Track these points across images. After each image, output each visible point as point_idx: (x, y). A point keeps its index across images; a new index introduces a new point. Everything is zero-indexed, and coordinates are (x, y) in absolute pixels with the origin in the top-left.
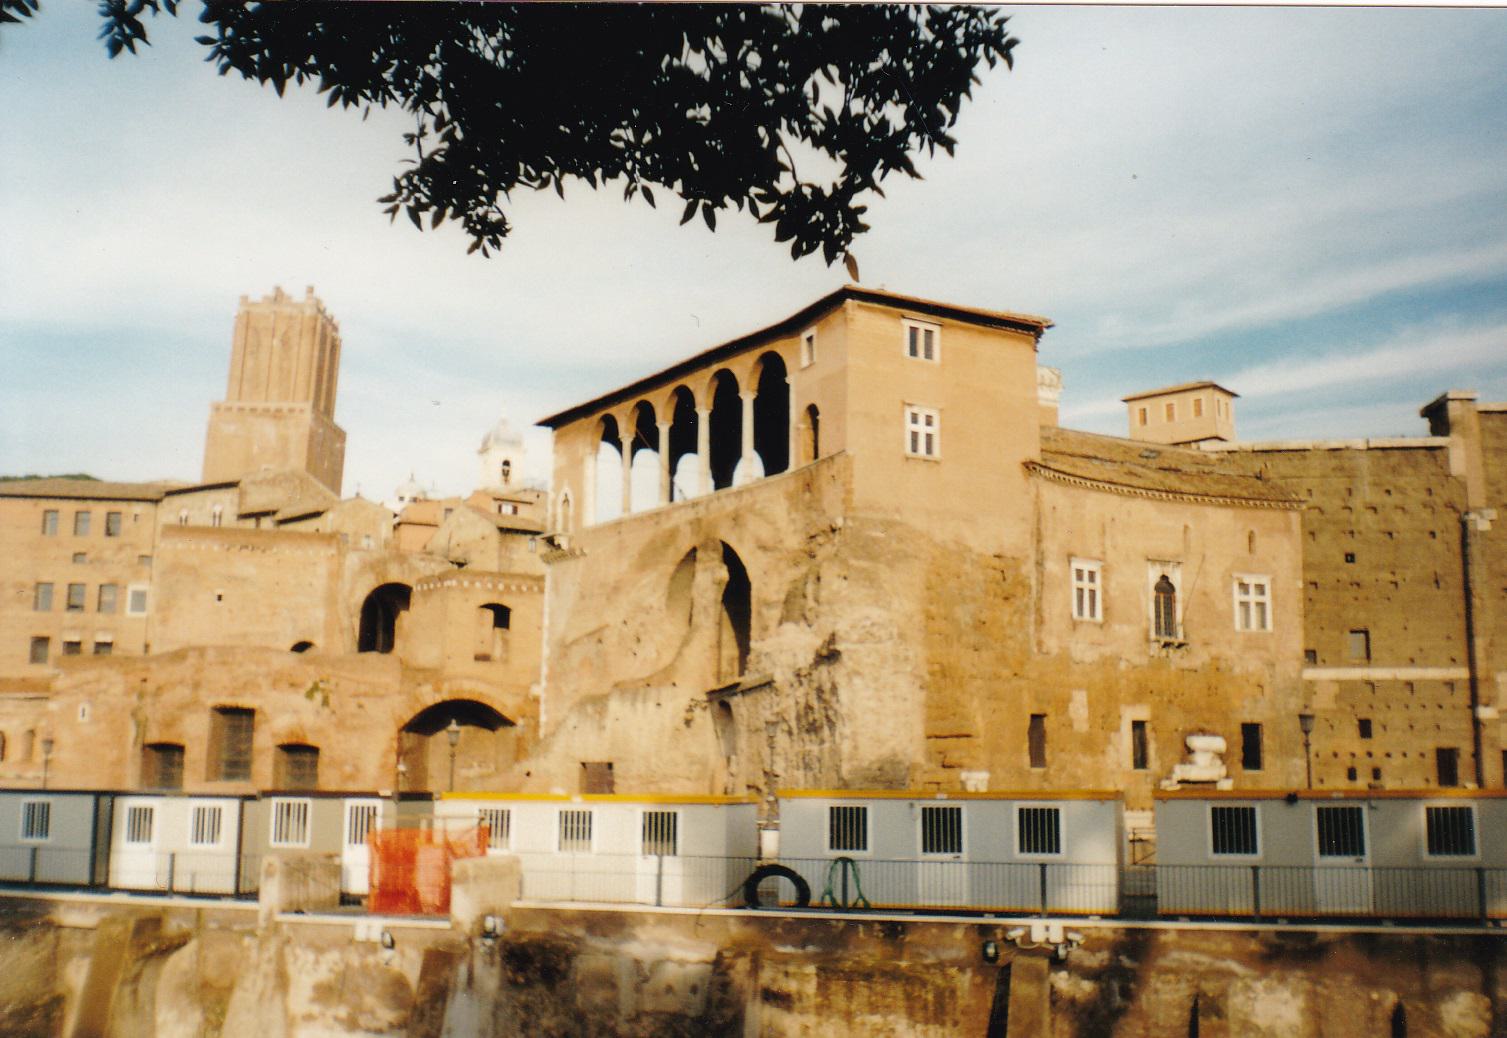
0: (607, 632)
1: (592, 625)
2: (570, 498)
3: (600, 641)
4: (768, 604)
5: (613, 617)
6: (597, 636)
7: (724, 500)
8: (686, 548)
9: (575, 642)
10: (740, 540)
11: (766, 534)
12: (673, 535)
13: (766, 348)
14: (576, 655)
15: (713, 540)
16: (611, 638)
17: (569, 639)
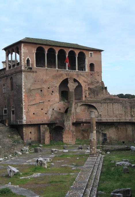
0: (43, 89)
1: (39, 87)
2: (30, 59)
3: (41, 91)
4: (86, 90)
5: (45, 86)
6: (40, 90)
7: (73, 72)
8: (66, 78)
9: (34, 90)
10: (80, 80)
11: (86, 80)
12: (62, 75)
13: (82, 51)
14: (34, 93)
15: (72, 78)
16: (45, 91)
17: (31, 89)
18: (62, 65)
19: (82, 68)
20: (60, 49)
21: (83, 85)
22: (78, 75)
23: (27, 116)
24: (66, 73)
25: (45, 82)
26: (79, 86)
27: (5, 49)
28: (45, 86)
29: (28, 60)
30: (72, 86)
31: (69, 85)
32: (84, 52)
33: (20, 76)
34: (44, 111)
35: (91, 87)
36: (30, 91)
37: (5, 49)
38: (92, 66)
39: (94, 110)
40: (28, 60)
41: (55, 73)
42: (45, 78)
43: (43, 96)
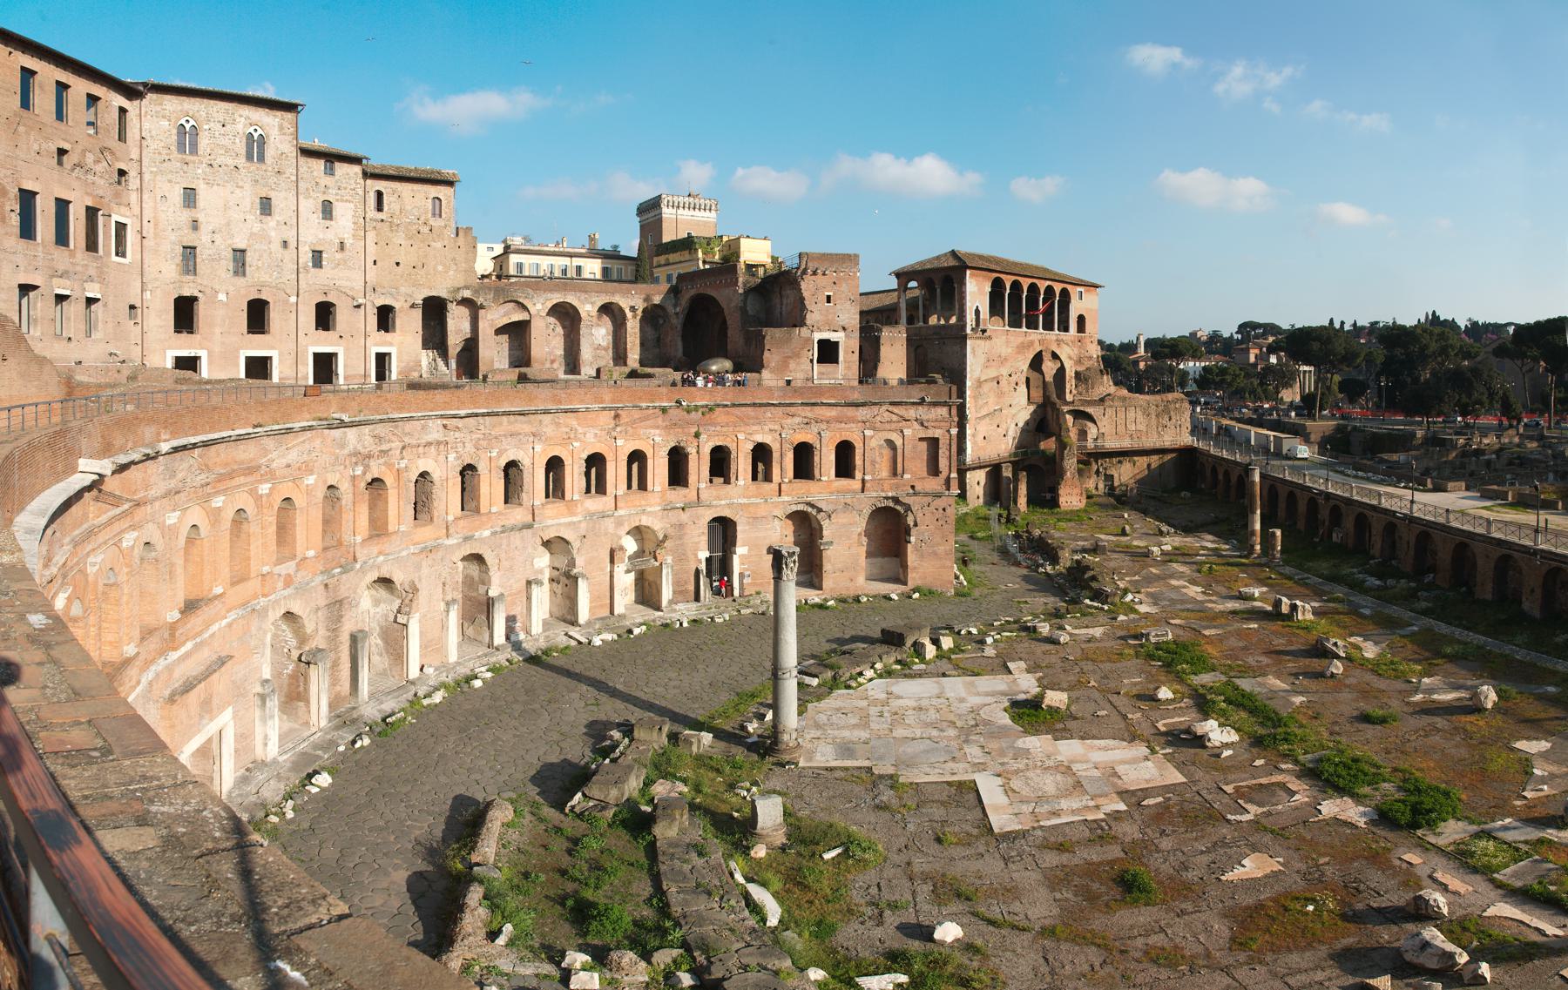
12: (1031, 343)
14: (986, 388)
18: (1032, 325)
19: (1065, 327)
20: (1030, 281)
21: (1068, 365)
22: (1059, 342)
23: (974, 443)
24: (1038, 338)
25: (1003, 361)
26: (1061, 371)
27: (898, 275)
28: (1005, 371)
29: (977, 312)
30: (1049, 368)
31: (1044, 368)
32: (1069, 287)
33: (957, 348)
34: (1001, 431)
35: (1080, 369)
36: (979, 383)
37: (898, 275)
38: (1081, 319)
39: (1090, 424)
40: (977, 312)
41: (1021, 339)
42: (1006, 351)
43: (1001, 395)
